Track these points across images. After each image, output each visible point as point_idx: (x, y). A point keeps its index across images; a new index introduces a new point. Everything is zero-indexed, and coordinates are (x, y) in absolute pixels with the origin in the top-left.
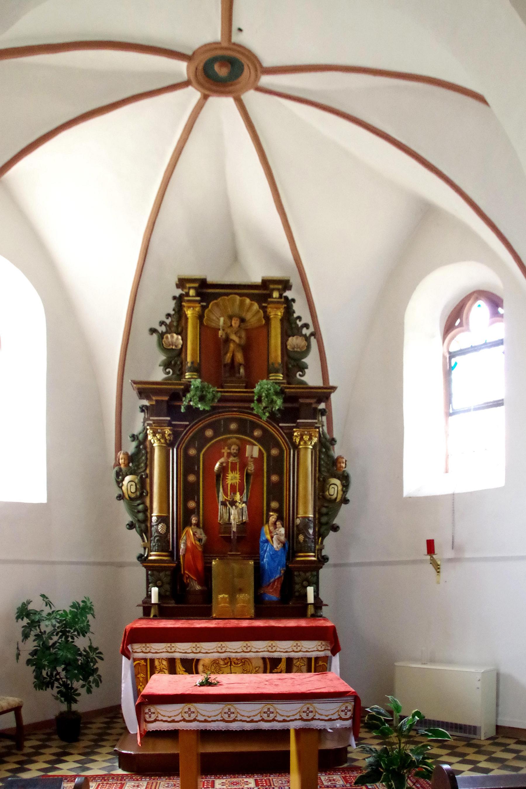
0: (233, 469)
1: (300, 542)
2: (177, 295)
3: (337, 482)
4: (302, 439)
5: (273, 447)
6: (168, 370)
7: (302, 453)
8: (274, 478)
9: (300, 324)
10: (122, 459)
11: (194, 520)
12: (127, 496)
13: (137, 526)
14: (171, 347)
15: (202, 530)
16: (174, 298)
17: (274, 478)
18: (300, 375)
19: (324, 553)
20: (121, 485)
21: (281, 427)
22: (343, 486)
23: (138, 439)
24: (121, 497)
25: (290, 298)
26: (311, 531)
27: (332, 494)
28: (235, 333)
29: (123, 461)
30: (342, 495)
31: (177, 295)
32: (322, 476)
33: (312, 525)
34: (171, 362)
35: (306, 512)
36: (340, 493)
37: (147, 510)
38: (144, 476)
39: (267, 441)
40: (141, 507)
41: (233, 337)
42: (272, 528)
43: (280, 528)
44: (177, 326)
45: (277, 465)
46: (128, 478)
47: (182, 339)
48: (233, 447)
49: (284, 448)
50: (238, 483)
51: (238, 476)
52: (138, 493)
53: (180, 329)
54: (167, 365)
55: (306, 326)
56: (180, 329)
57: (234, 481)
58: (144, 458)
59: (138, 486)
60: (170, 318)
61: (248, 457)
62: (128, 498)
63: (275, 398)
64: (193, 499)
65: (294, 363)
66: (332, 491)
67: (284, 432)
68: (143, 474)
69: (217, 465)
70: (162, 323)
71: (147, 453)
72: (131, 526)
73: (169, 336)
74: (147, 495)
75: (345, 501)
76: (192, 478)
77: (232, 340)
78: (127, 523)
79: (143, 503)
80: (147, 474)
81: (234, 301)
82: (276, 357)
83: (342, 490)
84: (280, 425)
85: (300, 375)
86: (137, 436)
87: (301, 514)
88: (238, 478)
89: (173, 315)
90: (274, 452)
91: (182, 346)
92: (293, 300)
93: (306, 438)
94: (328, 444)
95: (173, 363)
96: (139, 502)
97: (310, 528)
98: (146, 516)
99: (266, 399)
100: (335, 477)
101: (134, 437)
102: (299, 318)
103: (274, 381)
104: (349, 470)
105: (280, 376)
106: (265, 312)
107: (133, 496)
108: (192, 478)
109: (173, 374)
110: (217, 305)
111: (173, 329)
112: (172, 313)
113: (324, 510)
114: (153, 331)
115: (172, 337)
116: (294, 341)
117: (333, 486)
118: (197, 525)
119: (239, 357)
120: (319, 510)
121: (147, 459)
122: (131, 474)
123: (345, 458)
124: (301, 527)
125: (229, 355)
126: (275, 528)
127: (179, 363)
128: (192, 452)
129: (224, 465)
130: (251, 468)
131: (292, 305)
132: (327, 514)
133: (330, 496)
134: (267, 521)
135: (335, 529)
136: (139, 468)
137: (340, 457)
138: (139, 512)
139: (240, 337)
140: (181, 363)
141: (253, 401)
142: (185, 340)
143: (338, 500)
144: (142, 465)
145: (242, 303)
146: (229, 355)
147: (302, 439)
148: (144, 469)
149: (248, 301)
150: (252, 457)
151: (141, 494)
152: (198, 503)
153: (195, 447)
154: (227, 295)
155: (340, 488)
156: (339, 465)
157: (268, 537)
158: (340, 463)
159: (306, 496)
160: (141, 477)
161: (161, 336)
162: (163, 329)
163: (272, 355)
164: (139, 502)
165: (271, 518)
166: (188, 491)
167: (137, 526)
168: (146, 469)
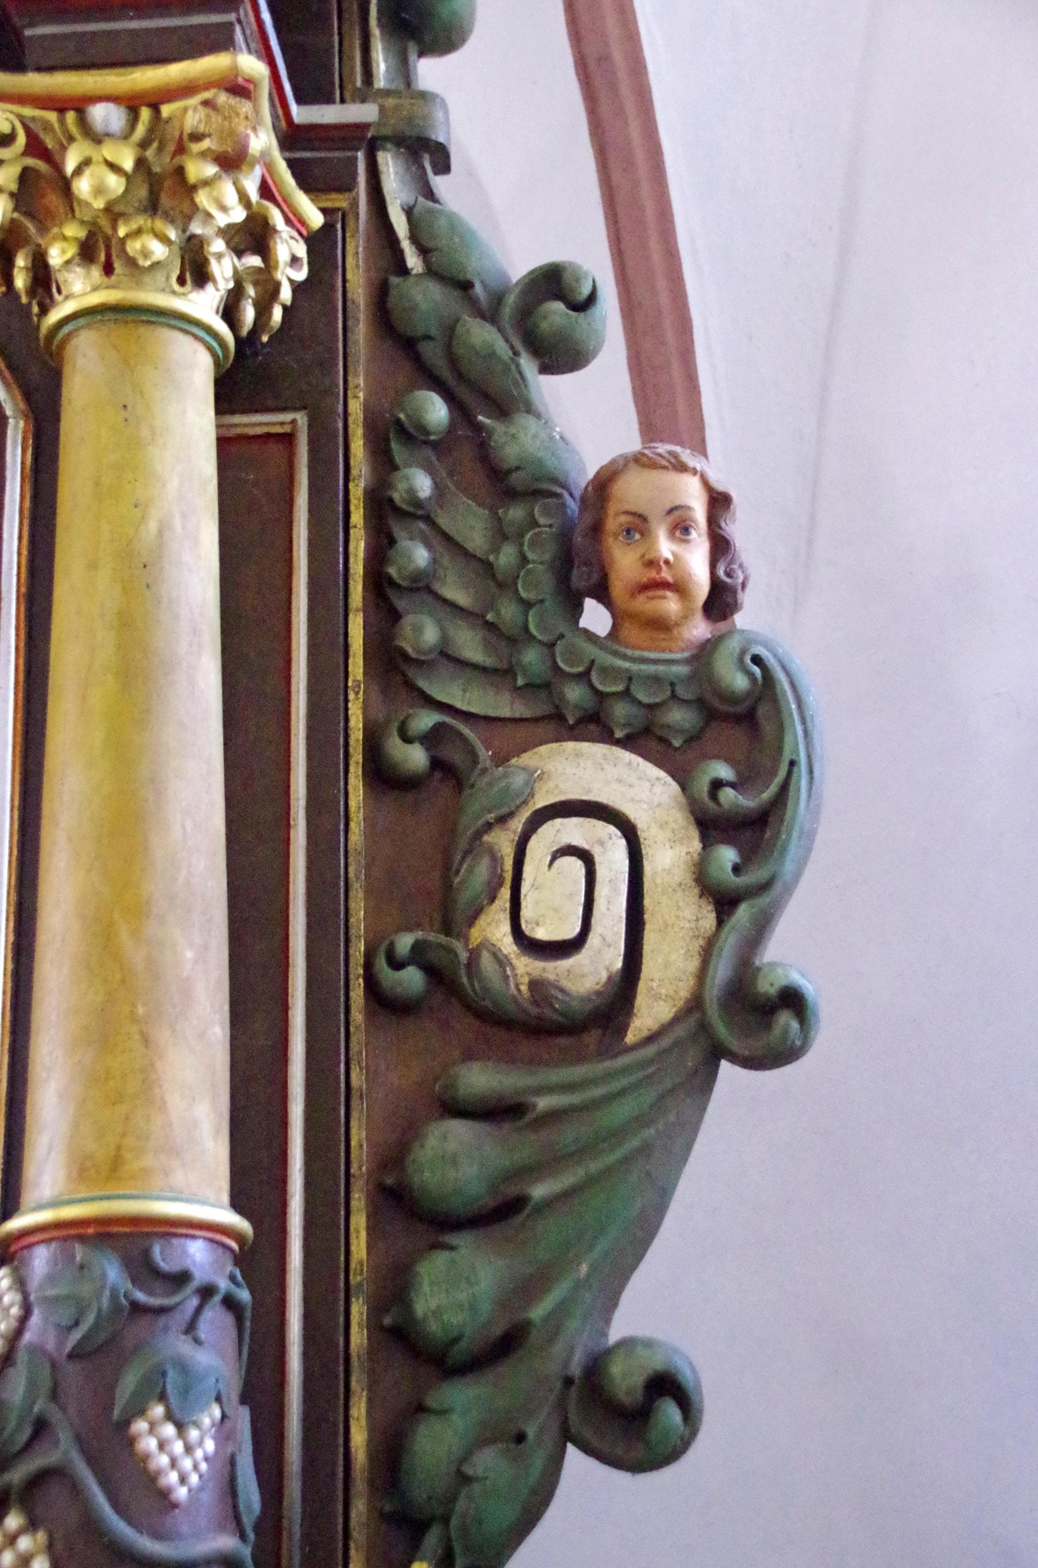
22: (711, 826)
27: (571, 930)
33: (211, 1353)
66: (551, 900)
75: (756, 1020)
100: (594, 725)
113: (456, 1158)
132: (501, 1212)
135: (639, 1417)
143: (652, 1011)
155: (671, 853)
156: (625, 563)
158: (638, 526)
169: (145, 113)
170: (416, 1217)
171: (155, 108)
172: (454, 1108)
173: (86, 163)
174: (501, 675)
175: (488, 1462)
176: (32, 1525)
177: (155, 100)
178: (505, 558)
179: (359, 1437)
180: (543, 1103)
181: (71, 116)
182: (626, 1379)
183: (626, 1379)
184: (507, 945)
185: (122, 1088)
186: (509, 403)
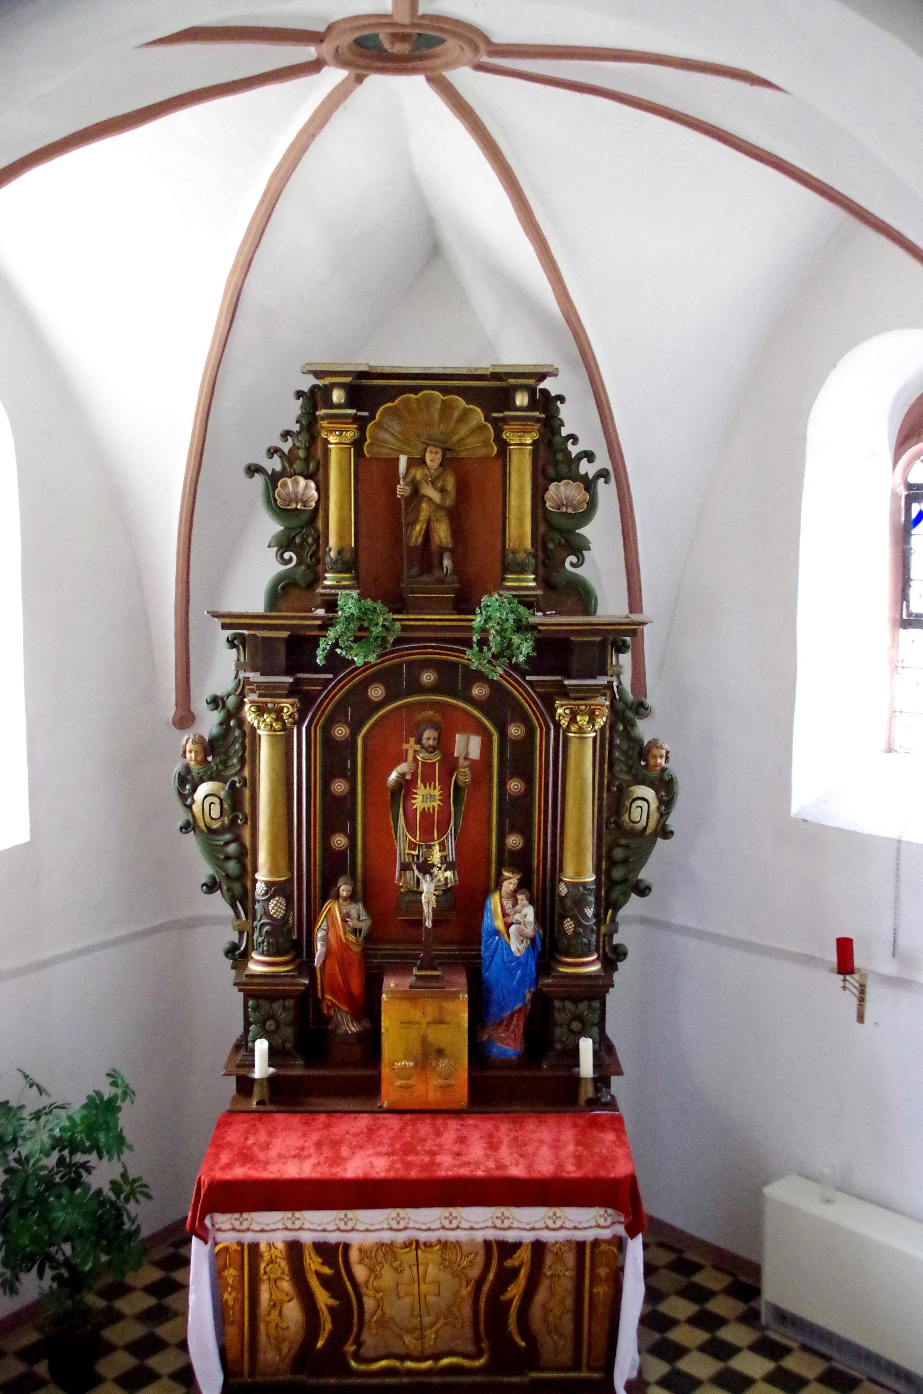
0: (428, 780)
1: (565, 934)
2: (306, 389)
3: (648, 792)
4: (573, 720)
5: (511, 722)
6: (287, 555)
7: (573, 747)
8: (515, 786)
9: (574, 450)
10: (190, 752)
11: (344, 889)
12: (202, 825)
13: (225, 888)
14: (293, 506)
15: (360, 906)
16: (299, 394)
17: (515, 786)
18: (572, 565)
19: (617, 939)
20: (189, 801)
22: (661, 801)
23: (224, 706)
24: (187, 827)
25: (553, 394)
26: (590, 912)
28: (433, 483)
29: (193, 755)
30: (659, 821)
31: (306, 389)
32: (617, 783)
33: (592, 899)
34: (294, 537)
35: (579, 874)
36: (655, 816)
37: (246, 858)
38: (238, 785)
39: (500, 707)
40: (232, 848)
41: (429, 491)
42: (508, 905)
43: (524, 906)
44: (307, 460)
45: (519, 759)
46: (204, 789)
47: (318, 490)
48: (426, 735)
51: (437, 793)
52: (226, 820)
53: (312, 466)
54: (284, 544)
55: (589, 456)
56: (312, 466)
57: (428, 805)
58: (237, 746)
59: (226, 806)
60: (289, 438)
62: (204, 829)
63: (516, 639)
64: (343, 831)
65: (559, 536)
66: (636, 814)
67: (535, 692)
68: (236, 779)
69: (394, 776)
70: (273, 452)
71: (244, 734)
72: (211, 887)
73: (289, 481)
74: (246, 823)
75: (666, 833)
76: (339, 787)
77: (424, 496)
78: (204, 880)
79: (237, 839)
80: (245, 780)
81: (429, 402)
82: (521, 536)
83: (658, 808)
84: (528, 678)
85: (572, 565)
86: (222, 699)
87: (569, 875)
88: (438, 798)
89: (298, 433)
90: (515, 731)
91: (317, 503)
92: (561, 399)
93: (583, 720)
94: (629, 714)
95: (298, 540)
96: (228, 837)
97: (588, 905)
98: (243, 867)
99: (499, 638)
100: (643, 782)
101: (216, 702)
102: (574, 438)
103: (514, 593)
104: (675, 768)
105: (529, 580)
106: (498, 431)
107: (216, 825)
108: (339, 787)
109: (299, 563)
110: (394, 412)
111: (298, 466)
112: (296, 428)
113: (619, 853)
114: (253, 470)
115: (296, 483)
116: (561, 492)
117: (639, 803)
118: (352, 898)
119: (442, 533)
120: (610, 850)
121: (244, 748)
122: (211, 779)
123: (666, 746)
124: (569, 903)
125: (419, 528)
126: (515, 903)
127: (310, 540)
128: (341, 732)
129: (408, 777)
130: (464, 775)
131: (558, 410)
132: (625, 861)
133: (631, 824)
134: (499, 886)
135: (643, 890)
136: (226, 767)
137: (654, 743)
138: (228, 858)
139: (442, 491)
140: (317, 540)
141: (468, 643)
142: (323, 489)
143: (649, 831)
144: (235, 761)
145: (447, 408)
146: (419, 528)
147: (573, 720)
148: (238, 768)
149: (462, 402)
150: (466, 758)
151: (233, 821)
152: (352, 838)
154: (415, 390)
156: (652, 762)
157: (499, 924)
158: (655, 757)
159: (580, 836)
160: (234, 783)
161: (274, 479)
162: (275, 464)
163: (512, 531)
164: (228, 837)
165: (505, 884)
166: (336, 814)
167: (225, 888)
168: (242, 769)
170: (613, 863)
172: (619, 846)
174: (629, 772)
175: (621, 898)
178: (631, 752)
179: (603, 893)
180: (633, 846)
182: (642, 886)
183: (642, 886)
184: (627, 819)
185: (580, 862)
186: (633, 725)
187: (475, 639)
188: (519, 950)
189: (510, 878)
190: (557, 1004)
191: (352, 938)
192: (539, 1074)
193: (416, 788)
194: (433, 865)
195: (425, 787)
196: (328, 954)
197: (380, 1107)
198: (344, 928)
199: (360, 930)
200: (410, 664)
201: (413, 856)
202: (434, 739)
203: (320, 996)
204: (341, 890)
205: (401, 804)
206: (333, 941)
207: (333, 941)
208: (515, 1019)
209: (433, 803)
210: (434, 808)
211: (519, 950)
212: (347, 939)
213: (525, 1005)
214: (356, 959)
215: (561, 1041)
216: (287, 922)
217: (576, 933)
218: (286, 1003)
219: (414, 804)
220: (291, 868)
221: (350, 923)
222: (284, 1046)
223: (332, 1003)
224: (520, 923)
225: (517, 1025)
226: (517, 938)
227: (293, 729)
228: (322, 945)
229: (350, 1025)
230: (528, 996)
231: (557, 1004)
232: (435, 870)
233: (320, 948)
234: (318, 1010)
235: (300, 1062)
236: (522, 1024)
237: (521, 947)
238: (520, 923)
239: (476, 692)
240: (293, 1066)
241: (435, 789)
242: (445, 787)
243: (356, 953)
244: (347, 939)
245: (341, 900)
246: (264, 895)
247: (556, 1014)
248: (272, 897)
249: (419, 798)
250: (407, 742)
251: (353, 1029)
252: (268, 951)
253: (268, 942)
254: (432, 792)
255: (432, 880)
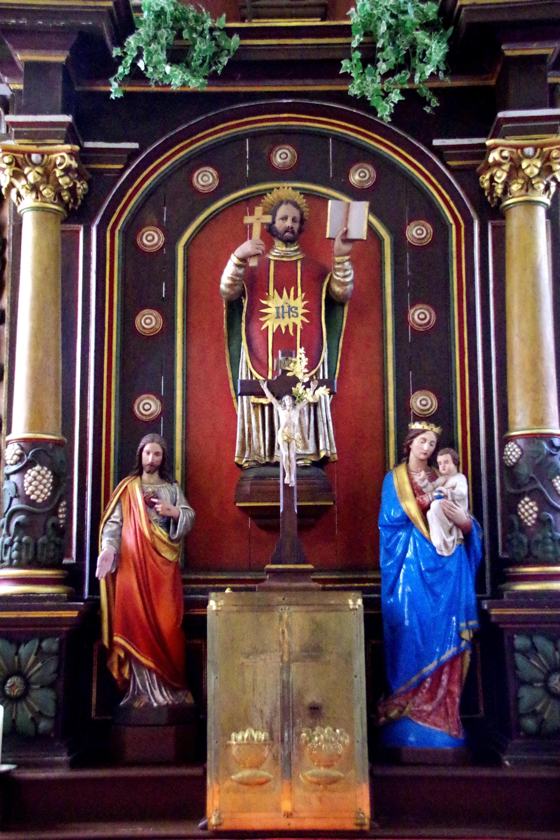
1: (523, 528)
5: (410, 221)
8: (420, 315)
17: (420, 315)
21: (438, 151)
39: (392, 198)
42: (420, 477)
43: (449, 474)
45: (425, 274)
49: (451, 221)
50: (299, 326)
51: (299, 303)
61: (332, 239)
67: (448, 167)
76: (148, 321)
84: (436, 142)
87: (521, 422)
88: (301, 311)
90: (418, 232)
118: (164, 470)
124: (524, 470)
128: (151, 238)
134: (403, 455)
153: (159, 226)
157: (411, 507)
159: (536, 361)
165: (416, 442)
169: (539, 150)
171: (542, 149)
173: (528, 166)
176: (532, 500)
177: (542, 146)
181: (519, 151)
187: (355, 44)
188: (445, 543)
189: (424, 431)
190: (520, 642)
191: (160, 532)
192: (499, 773)
193: (265, 299)
194: (295, 380)
195: (281, 295)
196: (120, 557)
197: (205, 828)
198: (147, 514)
199: (176, 524)
200: (255, 136)
201: (263, 406)
202: (294, 220)
203: (106, 642)
204: (144, 454)
205: (243, 325)
206: (130, 540)
207: (130, 540)
208: (445, 678)
209: (293, 320)
210: (295, 326)
211: (445, 543)
212: (152, 533)
213: (459, 655)
214: (167, 574)
215: (534, 714)
216: (55, 512)
217: (542, 522)
218: (44, 644)
219: (263, 323)
220: (68, 430)
221: (159, 507)
222: (37, 726)
223: (128, 654)
224: (446, 497)
225: (449, 693)
226: (442, 524)
227: (78, 232)
228: (110, 543)
229: (157, 693)
230: (466, 635)
231: (520, 642)
232: (299, 388)
233: (106, 546)
234: (105, 673)
235: (63, 758)
236: (456, 690)
237: (450, 540)
238: (446, 497)
239: (357, 177)
240: (52, 765)
241: (296, 297)
242: (312, 297)
243: (167, 562)
244: (152, 533)
245: (145, 476)
246: (16, 463)
247: (520, 660)
248: (30, 465)
249: (272, 310)
250: (252, 213)
251: (160, 699)
252: (19, 558)
253: (20, 542)
254: (292, 303)
255: (294, 405)
